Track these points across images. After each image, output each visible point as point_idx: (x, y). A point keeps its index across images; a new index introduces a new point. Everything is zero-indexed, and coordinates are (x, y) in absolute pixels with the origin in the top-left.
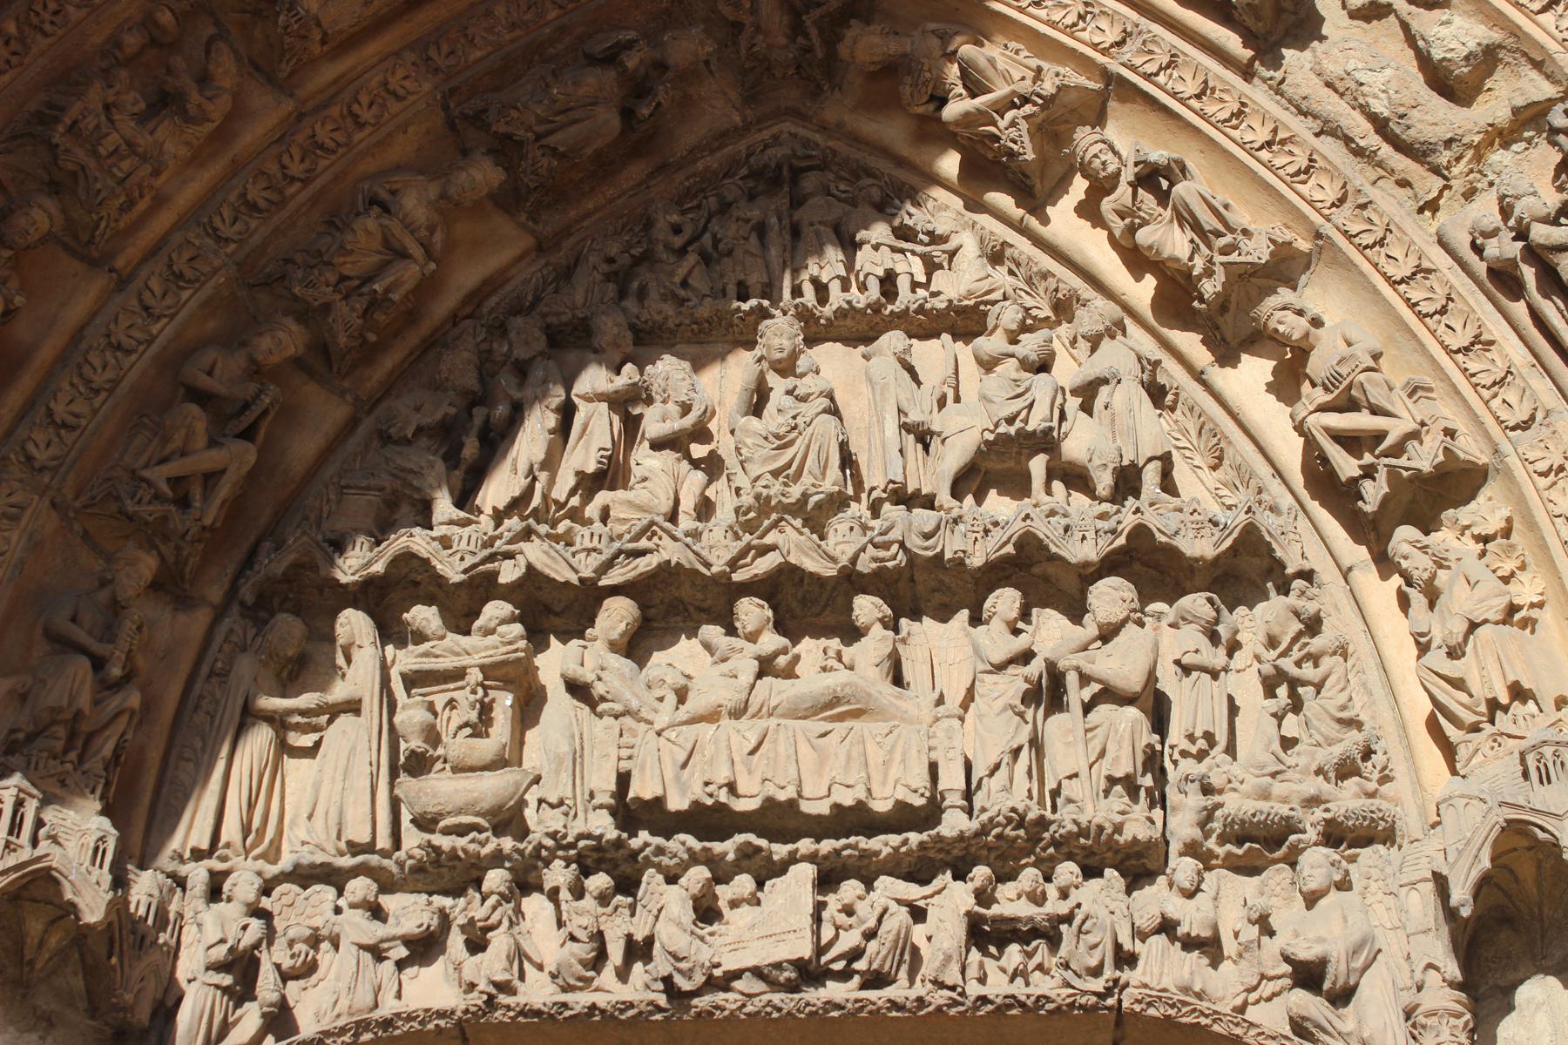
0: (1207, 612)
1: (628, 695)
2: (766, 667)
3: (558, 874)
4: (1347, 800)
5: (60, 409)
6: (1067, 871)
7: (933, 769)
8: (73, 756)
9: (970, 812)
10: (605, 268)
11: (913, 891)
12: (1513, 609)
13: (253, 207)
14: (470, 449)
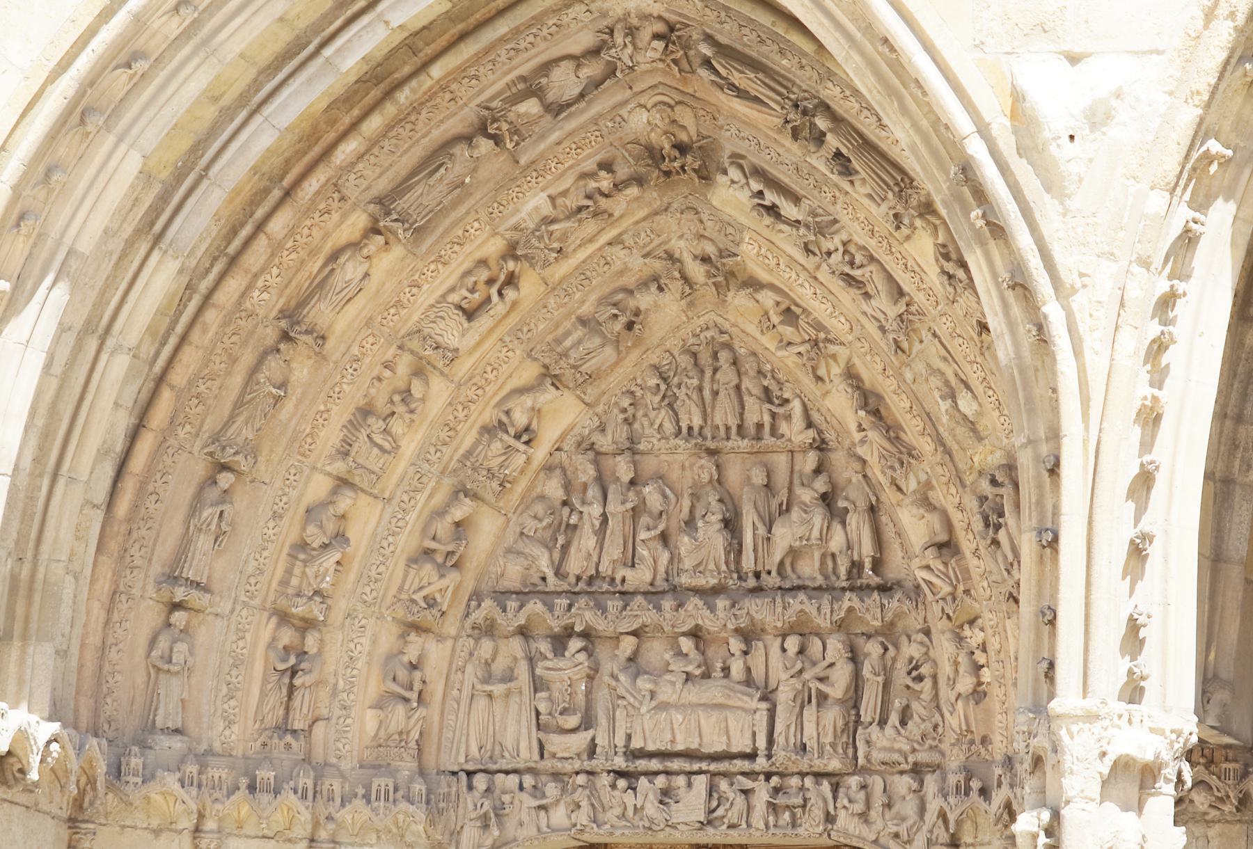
1: (628, 696)
3: (605, 780)
4: (923, 757)
5: (373, 574)
6: (808, 782)
7: (754, 734)
8: (403, 744)
9: (769, 757)
10: (622, 416)
11: (748, 783)
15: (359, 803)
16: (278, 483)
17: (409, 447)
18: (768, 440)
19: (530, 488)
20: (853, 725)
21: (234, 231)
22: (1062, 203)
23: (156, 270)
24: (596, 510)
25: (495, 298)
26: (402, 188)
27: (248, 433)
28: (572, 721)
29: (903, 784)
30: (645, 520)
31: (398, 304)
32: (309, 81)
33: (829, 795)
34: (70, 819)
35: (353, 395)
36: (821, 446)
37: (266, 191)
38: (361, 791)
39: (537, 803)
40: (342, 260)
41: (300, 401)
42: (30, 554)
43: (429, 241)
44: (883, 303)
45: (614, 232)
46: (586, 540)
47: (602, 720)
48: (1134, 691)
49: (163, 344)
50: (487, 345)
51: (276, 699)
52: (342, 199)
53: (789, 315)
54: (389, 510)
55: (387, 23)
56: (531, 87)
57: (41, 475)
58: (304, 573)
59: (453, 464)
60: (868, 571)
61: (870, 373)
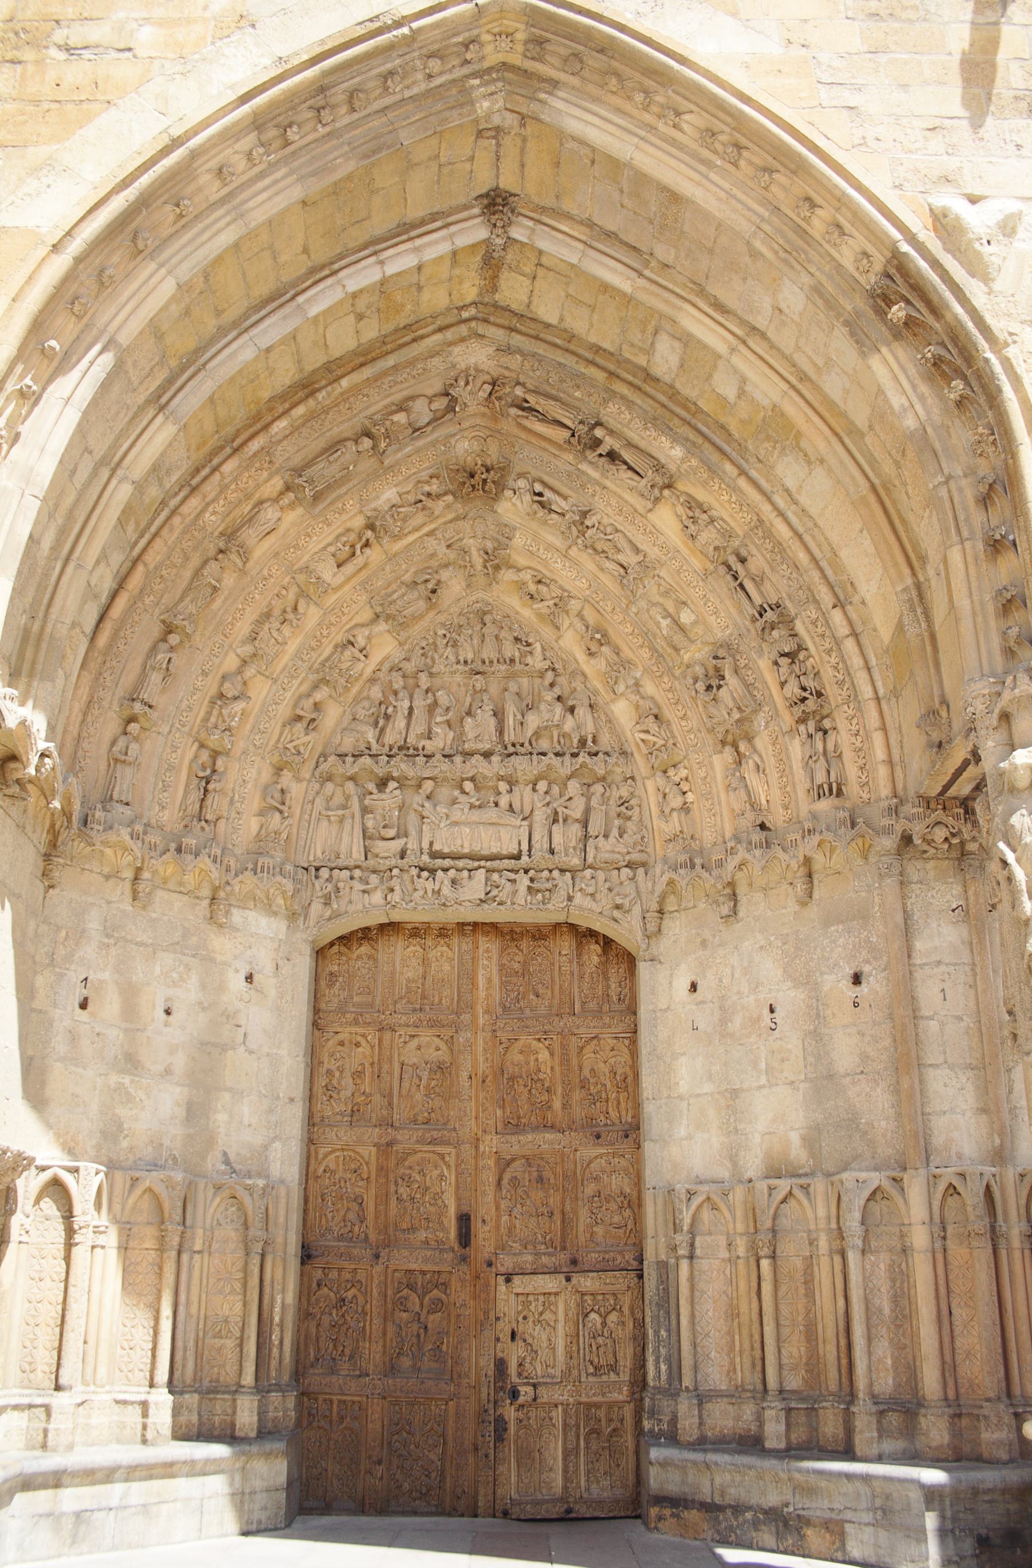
0: (602, 790)
2: (472, 807)
3: (414, 872)
4: (636, 857)
6: (556, 873)
9: (530, 856)
11: (512, 876)
12: (685, 803)
13: (313, 649)
14: (381, 722)
15: (248, 874)
16: (207, 652)
17: (292, 647)
18: (518, 667)
19: (360, 692)
21: (198, 470)
22: (986, 285)
23: (159, 429)
24: (406, 704)
25: (358, 552)
26: (310, 463)
27: (192, 609)
28: (391, 833)
30: (439, 710)
31: (296, 547)
32: (285, 318)
33: (570, 882)
34: (45, 855)
37: (222, 448)
38: (250, 866)
39: (364, 887)
40: (265, 505)
41: (226, 599)
42: (41, 615)
43: (321, 506)
45: (432, 526)
46: (400, 723)
47: (413, 832)
49: (142, 536)
50: (346, 588)
51: (195, 796)
52: (270, 462)
54: (274, 687)
55: (344, 286)
57: (56, 559)
58: (221, 713)
59: (316, 666)
60: (590, 743)
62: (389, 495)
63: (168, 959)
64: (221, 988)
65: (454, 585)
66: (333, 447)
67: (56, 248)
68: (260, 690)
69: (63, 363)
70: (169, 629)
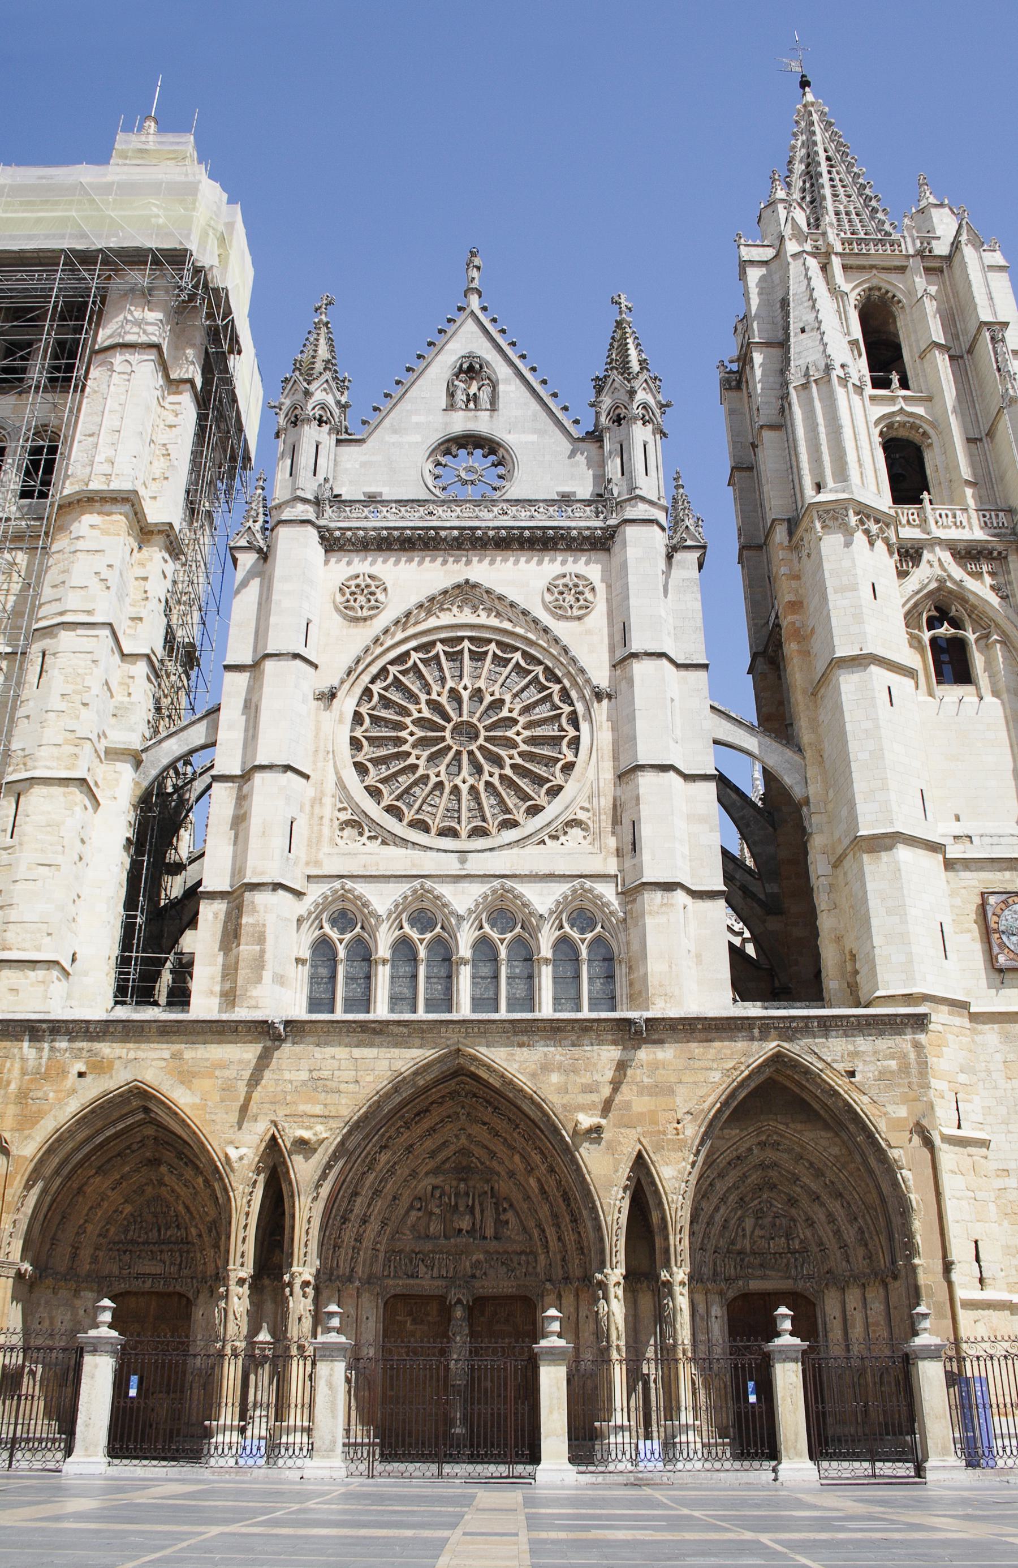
20: (180, 1269)
26: (103, 1165)
29: (189, 1280)
35: (90, 1204)
36: (177, 1216)
44: (191, 1190)
46: (131, 1233)
48: (242, 1265)
53: (173, 1191)
56: (129, 1147)
61: (188, 1202)
62: (127, 1169)
63: (62, 1308)
64: (77, 1314)
65: (149, 1190)
66: (110, 1160)
67: (31, 1161)
68: (90, 1227)
69: (33, 1186)
70: (64, 1217)
